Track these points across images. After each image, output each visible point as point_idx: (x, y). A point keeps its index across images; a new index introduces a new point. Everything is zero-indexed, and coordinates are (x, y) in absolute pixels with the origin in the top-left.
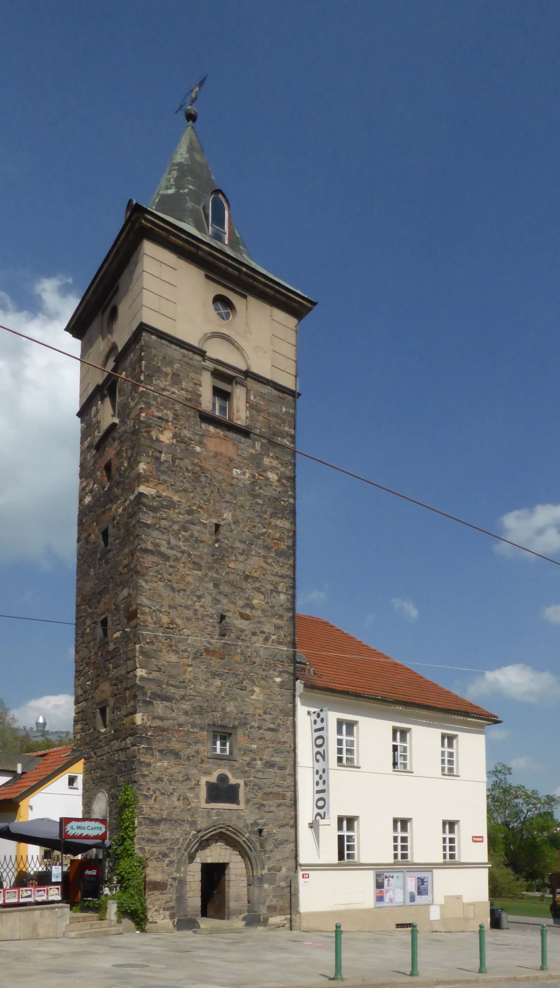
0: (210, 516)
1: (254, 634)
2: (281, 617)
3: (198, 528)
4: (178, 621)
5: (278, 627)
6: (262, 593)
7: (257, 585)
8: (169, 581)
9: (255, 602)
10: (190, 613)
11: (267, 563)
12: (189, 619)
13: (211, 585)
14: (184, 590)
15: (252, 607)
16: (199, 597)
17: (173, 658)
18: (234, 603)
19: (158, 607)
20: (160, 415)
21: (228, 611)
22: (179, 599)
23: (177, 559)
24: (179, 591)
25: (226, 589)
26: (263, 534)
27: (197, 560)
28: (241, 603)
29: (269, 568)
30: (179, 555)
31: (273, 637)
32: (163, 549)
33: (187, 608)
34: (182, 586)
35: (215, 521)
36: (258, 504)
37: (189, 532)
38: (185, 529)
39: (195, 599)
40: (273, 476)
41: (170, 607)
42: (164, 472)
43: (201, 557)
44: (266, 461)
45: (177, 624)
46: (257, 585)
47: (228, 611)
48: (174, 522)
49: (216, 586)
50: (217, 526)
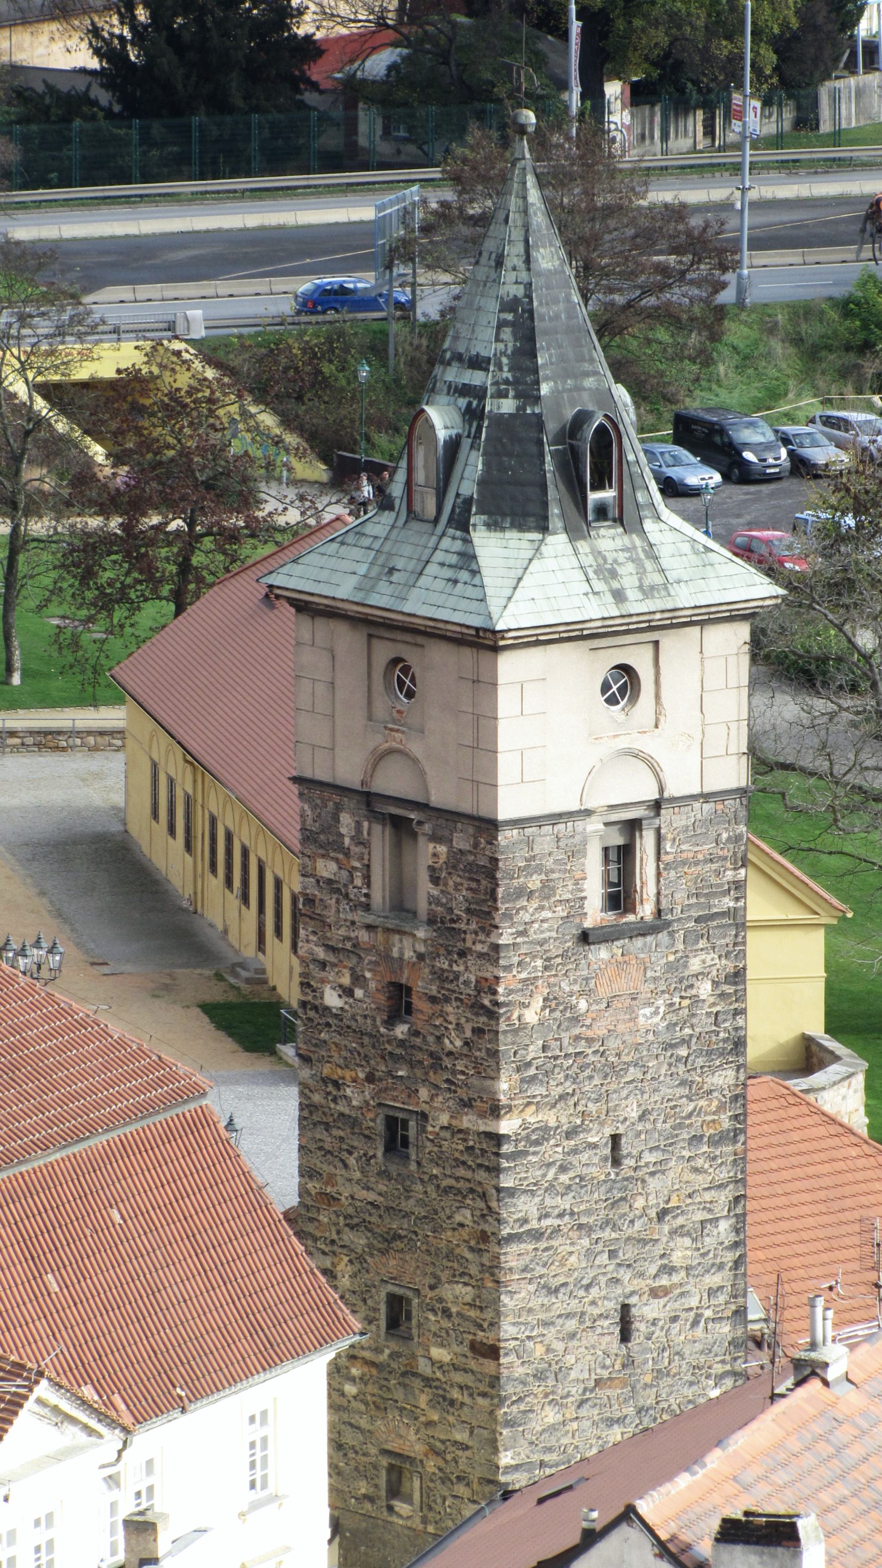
0: (602, 1124)
1: (674, 1319)
2: (721, 1267)
3: (584, 1157)
4: (559, 1346)
5: (712, 1292)
6: (688, 1234)
7: (680, 1221)
8: (541, 1277)
9: (677, 1258)
10: (572, 1325)
11: (696, 1170)
12: (572, 1336)
13: (604, 1258)
14: (565, 1284)
15: (669, 1270)
16: (588, 1287)
17: (551, 1416)
18: (641, 1275)
19: (527, 1333)
20: (524, 975)
21: (633, 1293)
22: (561, 1304)
23: (557, 1230)
24: (557, 1290)
25: (628, 1253)
26: (690, 1115)
27: (584, 1220)
28: (653, 1269)
29: (700, 1178)
30: (557, 1222)
31: (708, 1313)
32: (534, 1224)
33: (569, 1316)
34: (562, 1280)
35: (608, 1131)
36: (679, 1059)
37: (571, 1174)
38: (563, 1169)
39: (582, 1293)
40: (705, 989)
41: (546, 1324)
42: (533, 1079)
43: (588, 1212)
44: (695, 965)
45: (554, 1351)
46: (680, 1221)
47: (633, 1293)
48: (549, 1165)
49: (612, 1254)
50: (615, 1139)
